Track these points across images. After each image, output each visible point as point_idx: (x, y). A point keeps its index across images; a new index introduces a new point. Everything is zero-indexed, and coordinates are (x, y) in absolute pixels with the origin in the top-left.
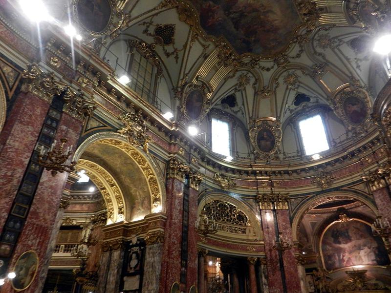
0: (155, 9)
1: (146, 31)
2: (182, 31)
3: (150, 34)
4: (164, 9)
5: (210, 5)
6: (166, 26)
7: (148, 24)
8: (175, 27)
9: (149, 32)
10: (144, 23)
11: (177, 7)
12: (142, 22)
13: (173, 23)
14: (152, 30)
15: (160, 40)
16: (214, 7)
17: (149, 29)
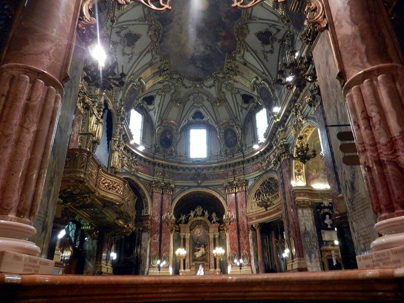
0: (252, 54)
1: (271, 52)
2: (254, 28)
3: (272, 47)
4: (249, 49)
5: (225, 18)
6: (260, 39)
7: (265, 53)
9: (271, 49)
10: (265, 57)
11: (243, 40)
14: (268, 48)
17: (269, 50)
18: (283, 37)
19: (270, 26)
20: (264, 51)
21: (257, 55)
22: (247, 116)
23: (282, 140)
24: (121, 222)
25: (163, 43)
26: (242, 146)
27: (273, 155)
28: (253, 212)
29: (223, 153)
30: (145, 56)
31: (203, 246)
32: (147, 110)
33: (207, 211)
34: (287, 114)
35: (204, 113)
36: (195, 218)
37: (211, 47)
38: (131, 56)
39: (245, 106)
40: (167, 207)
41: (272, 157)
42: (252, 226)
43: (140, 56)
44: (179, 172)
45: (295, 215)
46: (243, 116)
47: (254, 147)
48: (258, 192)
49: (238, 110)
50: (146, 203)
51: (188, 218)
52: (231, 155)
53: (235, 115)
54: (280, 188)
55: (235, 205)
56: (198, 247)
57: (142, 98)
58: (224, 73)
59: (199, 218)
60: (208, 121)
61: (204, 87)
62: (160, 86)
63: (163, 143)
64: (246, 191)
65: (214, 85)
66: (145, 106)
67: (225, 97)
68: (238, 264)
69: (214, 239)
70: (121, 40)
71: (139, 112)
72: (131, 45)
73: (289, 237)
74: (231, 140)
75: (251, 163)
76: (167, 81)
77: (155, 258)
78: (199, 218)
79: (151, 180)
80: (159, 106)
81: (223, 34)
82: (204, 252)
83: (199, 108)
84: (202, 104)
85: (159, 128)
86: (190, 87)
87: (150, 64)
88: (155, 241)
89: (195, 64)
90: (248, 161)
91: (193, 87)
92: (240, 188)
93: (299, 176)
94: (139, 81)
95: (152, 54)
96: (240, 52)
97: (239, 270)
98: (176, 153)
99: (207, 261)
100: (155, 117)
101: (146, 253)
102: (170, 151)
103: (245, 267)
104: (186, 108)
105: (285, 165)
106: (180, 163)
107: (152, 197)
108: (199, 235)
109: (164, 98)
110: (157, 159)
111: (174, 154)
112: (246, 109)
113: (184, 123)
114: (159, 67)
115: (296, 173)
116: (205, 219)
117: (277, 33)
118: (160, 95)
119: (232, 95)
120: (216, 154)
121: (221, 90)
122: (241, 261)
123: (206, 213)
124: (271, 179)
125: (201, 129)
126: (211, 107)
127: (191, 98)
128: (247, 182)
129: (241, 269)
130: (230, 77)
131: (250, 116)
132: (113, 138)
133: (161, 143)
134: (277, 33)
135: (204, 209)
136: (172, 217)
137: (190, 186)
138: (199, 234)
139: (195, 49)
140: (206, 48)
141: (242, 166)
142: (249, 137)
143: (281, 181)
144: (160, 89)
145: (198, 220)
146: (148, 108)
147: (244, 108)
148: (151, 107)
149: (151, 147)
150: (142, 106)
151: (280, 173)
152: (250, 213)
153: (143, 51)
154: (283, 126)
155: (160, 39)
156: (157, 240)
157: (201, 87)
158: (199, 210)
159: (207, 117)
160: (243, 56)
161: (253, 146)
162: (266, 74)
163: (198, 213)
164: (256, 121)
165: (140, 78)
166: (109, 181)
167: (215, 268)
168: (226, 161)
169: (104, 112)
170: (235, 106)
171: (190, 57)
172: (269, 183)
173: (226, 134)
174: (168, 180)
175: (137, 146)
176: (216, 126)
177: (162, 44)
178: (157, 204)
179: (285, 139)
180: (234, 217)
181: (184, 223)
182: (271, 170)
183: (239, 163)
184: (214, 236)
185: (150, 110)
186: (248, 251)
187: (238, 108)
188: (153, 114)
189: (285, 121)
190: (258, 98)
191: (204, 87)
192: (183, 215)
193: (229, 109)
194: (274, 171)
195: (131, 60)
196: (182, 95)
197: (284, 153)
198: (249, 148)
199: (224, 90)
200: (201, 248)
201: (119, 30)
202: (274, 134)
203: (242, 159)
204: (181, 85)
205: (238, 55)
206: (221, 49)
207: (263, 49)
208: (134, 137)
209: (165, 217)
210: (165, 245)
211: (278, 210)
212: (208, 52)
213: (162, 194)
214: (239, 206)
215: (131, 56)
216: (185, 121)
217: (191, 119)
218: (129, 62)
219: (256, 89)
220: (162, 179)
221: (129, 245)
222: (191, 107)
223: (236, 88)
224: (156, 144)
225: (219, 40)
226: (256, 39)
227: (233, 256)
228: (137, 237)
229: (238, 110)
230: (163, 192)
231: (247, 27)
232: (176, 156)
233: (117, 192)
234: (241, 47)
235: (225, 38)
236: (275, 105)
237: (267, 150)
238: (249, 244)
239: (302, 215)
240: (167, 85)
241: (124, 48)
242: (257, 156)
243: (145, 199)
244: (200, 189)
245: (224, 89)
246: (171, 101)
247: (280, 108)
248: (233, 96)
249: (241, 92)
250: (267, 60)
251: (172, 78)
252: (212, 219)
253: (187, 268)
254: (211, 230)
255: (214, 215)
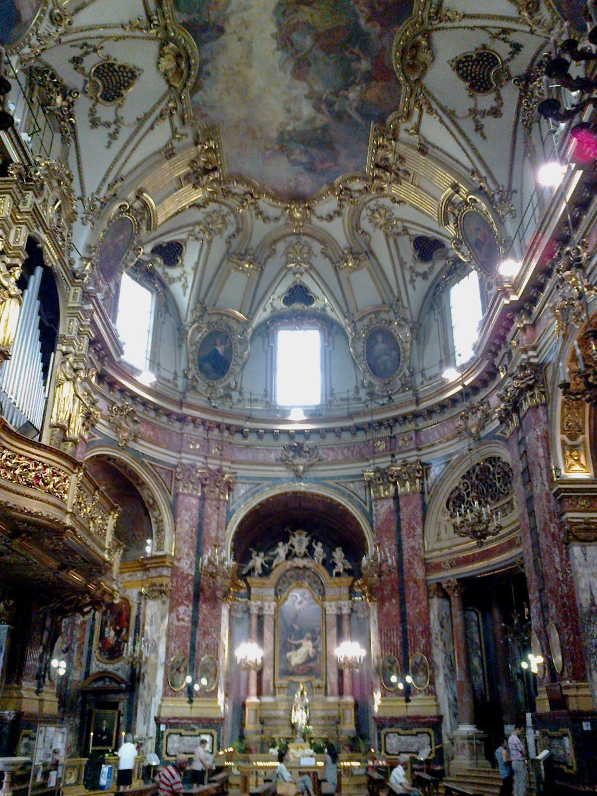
0: (441, 121)
3: (499, 98)
4: (434, 106)
5: (369, 20)
6: (464, 77)
7: (478, 117)
8: (453, 61)
9: (494, 104)
10: (479, 128)
11: (418, 81)
12: (475, 138)
13: (451, 69)
14: (486, 101)
15: (497, 77)
16: (361, 11)
17: (488, 108)
18: (529, 71)
19: (495, 37)
20: (473, 112)
21: (455, 124)
22: (426, 296)
23: (525, 351)
24: (76, 577)
25: (200, 93)
26: (412, 374)
27: (498, 396)
28: (441, 550)
29: (363, 394)
30: (152, 127)
31: (308, 635)
32: (166, 281)
33: (320, 544)
34: (541, 278)
35: (314, 289)
36: (289, 563)
37: (330, 105)
38: (113, 127)
39: (422, 267)
40: (213, 534)
41: (494, 400)
42: (439, 584)
43: (139, 129)
44: (246, 442)
45: (562, 560)
46: (415, 294)
47: (444, 376)
48: (457, 493)
49: (404, 278)
50: (159, 522)
51: (270, 563)
52: (383, 397)
53: (396, 294)
54: (517, 484)
55: (394, 528)
56: (295, 639)
57: (148, 249)
58: (365, 179)
59: (300, 562)
60: (324, 309)
61: (315, 220)
62: (198, 215)
63: (207, 365)
64: (422, 493)
65: (338, 213)
66: (159, 270)
67: (369, 246)
68: (401, 686)
69: (339, 618)
70: (86, 82)
71: (143, 285)
72: (113, 99)
73: (545, 621)
74: (385, 358)
75: (436, 418)
76: (215, 201)
77: (178, 670)
78: (300, 562)
79: (174, 461)
80: (195, 269)
81: (365, 65)
82: (311, 651)
83: (301, 274)
84: (309, 263)
85: (195, 325)
86: (277, 219)
87: (169, 153)
88: (182, 623)
89: (288, 157)
90: (430, 412)
91: (282, 221)
92: (408, 484)
93: (575, 453)
94: (138, 197)
95: (172, 124)
96: (408, 115)
97: (404, 704)
98: (241, 393)
99: (318, 676)
100: (184, 298)
101: (157, 657)
102: (224, 388)
103: (420, 696)
104: (265, 273)
105: (533, 420)
106: (249, 418)
107: (174, 510)
108: (298, 607)
109: (209, 248)
110: (190, 406)
111: (235, 395)
112: (425, 276)
113: (262, 315)
114: (193, 162)
115: (563, 443)
116: (315, 563)
117: (512, 54)
118: (197, 239)
119: (387, 236)
120: (345, 396)
121: (357, 227)
122: (409, 679)
123: (319, 549)
124: (493, 460)
125: (305, 330)
126: (333, 273)
127: (281, 247)
128: (425, 468)
129: (408, 700)
130: (382, 189)
131: (434, 294)
132: (59, 346)
133: (201, 369)
134: (512, 54)
135: (315, 539)
136: (225, 559)
137: (278, 478)
138: (300, 603)
139: (288, 111)
140: (318, 109)
141: (411, 426)
142: (432, 351)
143: (521, 466)
144: (198, 223)
145: (297, 567)
146: (166, 274)
147: (418, 274)
148: (174, 272)
149: (175, 379)
150: (151, 268)
151: (519, 443)
152: (434, 550)
153: (147, 116)
154: (529, 313)
155: (193, 80)
156: (187, 622)
157: (306, 219)
158: (300, 541)
159: (323, 301)
160: (417, 130)
161: (441, 373)
162: (479, 176)
163: (297, 550)
164: (450, 308)
165: (140, 192)
166: (26, 463)
167: (341, 693)
168: (372, 413)
169: (29, 268)
170: (394, 267)
171: (274, 135)
172: (485, 470)
173: (370, 341)
174: (218, 462)
175: (139, 372)
176: (343, 322)
177: (199, 96)
178: (187, 527)
179: (534, 348)
180: (392, 561)
181: (260, 575)
182: (492, 436)
183: (405, 417)
184: (340, 609)
185: (172, 280)
186: (428, 653)
187: (403, 274)
188: (181, 290)
189: (533, 301)
190: (458, 243)
191: (315, 220)
192: (258, 555)
193: (379, 274)
194: (500, 438)
195: (115, 138)
196: (255, 241)
197: (530, 388)
198: (430, 378)
199: (365, 225)
200: (304, 642)
201: (77, 52)
202: (503, 339)
203: (413, 408)
204: (254, 212)
205: (404, 125)
206: (357, 109)
207: (471, 103)
208: (124, 348)
209: (206, 562)
210: (206, 633)
211: (511, 545)
212: (322, 119)
213: (203, 498)
214: (404, 532)
215: (113, 127)
216: (265, 310)
217: (280, 305)
218: (109, 145)
219: (452, 219)
220: (202, 459)
221: (112, 633)
222: (280, 272)
223: (398, 219)
224: (189, 369)
225: (353, 83)
226: (454, 75)
227: (388, 664)
228: (134, 613)
229: (404, 278)
230: (203, 492)
231: (429, 40)
232: (239, 401)
233: (50, 492)
234: (412, 101)
235: (368, 78)
236: (506, 256)
237: (484, 382)
238: (430, 635)
239: (582, 561)
240: (214, 211)
241: (94, 106)
242: (454, 400)
243: (156, 513)
244: (302, 486)
245: (367, 220)
246: (228, 255)
247: (521, 263)
248: (391, 241)
249: (412, 232)
250: (482, 135)
251: (227, 193)
252: (334, 564)
253: (268, 694)
254: (330, 592)
255: (338, 554)
